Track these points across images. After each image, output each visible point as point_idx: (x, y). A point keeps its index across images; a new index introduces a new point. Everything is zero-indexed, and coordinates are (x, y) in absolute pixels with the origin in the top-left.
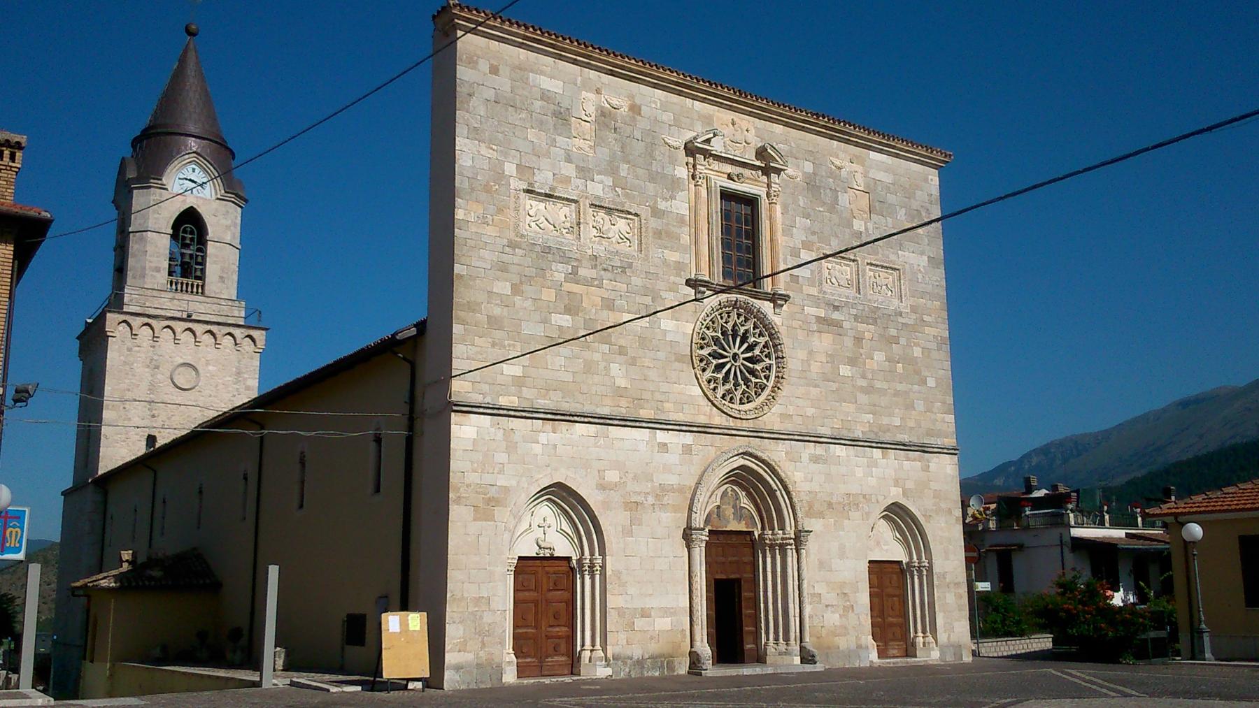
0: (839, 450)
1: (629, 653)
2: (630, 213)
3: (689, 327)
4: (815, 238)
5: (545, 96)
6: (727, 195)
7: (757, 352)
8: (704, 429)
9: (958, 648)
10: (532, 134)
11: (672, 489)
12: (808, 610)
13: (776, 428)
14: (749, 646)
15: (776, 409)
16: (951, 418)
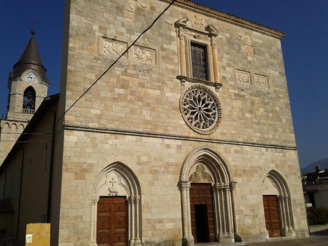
0: (247, 148)
1: (153, 240)
3: (179, 96)
4: (232, 63)
6: (193, 44)
7: (209, 107)
8: (186, 138)
9: (303, 231)
10: (106, 15)
11: (173, 165)
12: (237, 217)
13: (219, 138)
14: (212, 234)
15: (219, 130)
16: (293, 135)
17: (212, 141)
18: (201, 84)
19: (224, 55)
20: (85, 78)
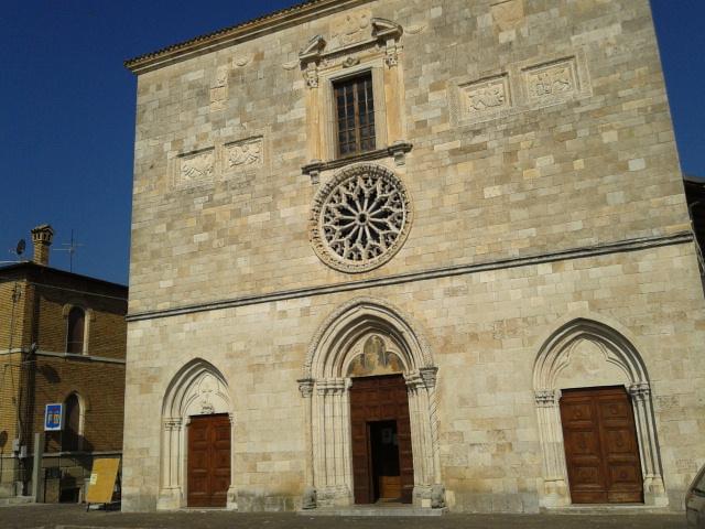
0: (483, 277)
1: (252, 491)
2: (255, 137)
3: (307, 208)
4: (447, 75)
5: (191, 86)
6: (338, 84)
8: (317, 291)
11: (291, 348)
13: (402, 271)
17: (379, 283)
18: (355, 165)
19: (424, 67)
20: (153, 236)
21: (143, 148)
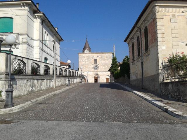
21: (79, 60)
